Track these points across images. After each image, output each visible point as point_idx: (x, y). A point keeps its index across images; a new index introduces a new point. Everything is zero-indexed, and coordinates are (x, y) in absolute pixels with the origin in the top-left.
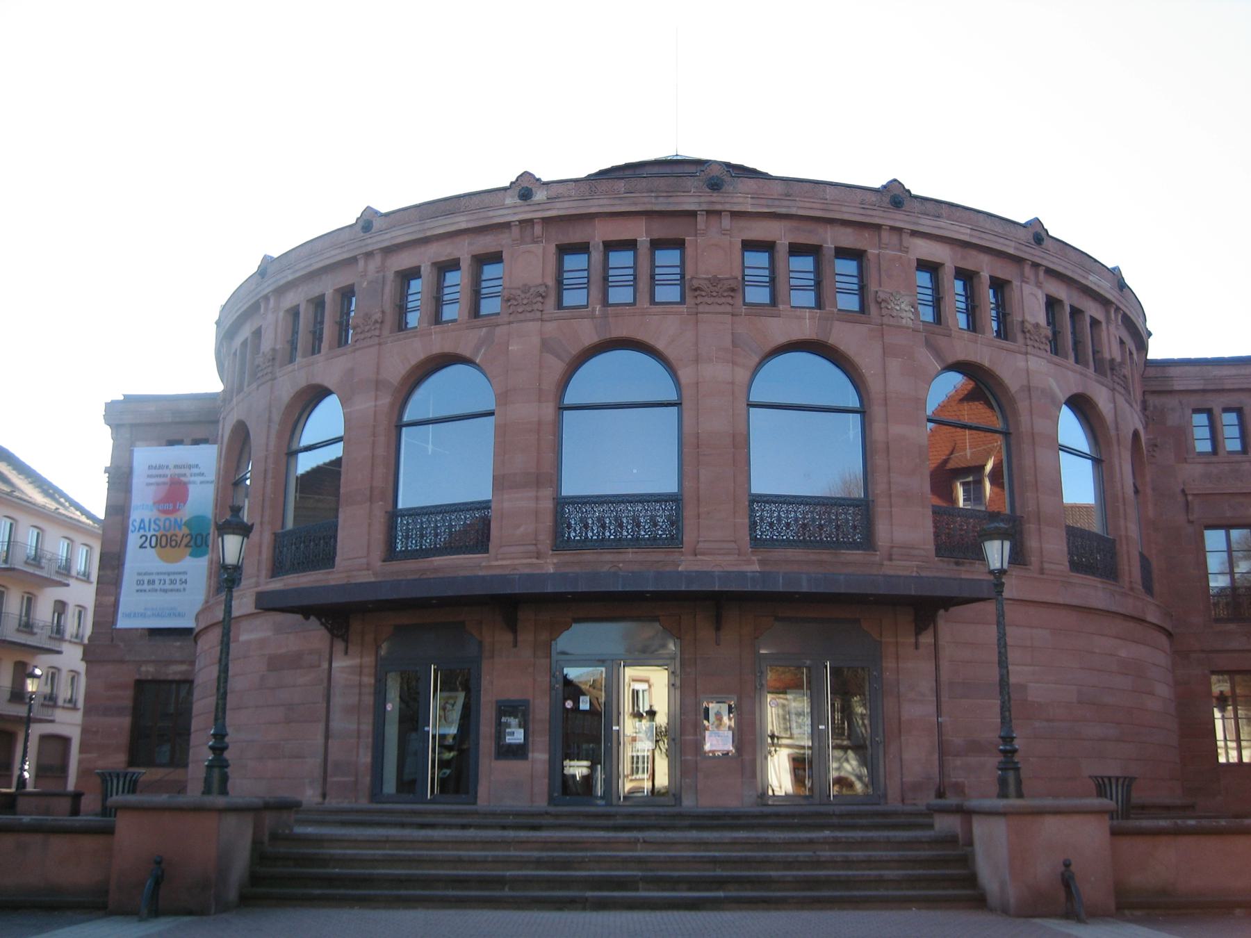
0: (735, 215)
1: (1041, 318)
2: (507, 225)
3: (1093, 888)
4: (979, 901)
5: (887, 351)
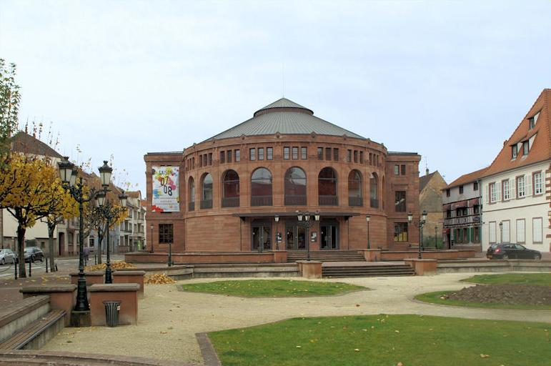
0: (317, 143)
1: (368, 158)
2: (274, 143)
3: (378, 259)
4: (365, 261)
5: (342, 168)
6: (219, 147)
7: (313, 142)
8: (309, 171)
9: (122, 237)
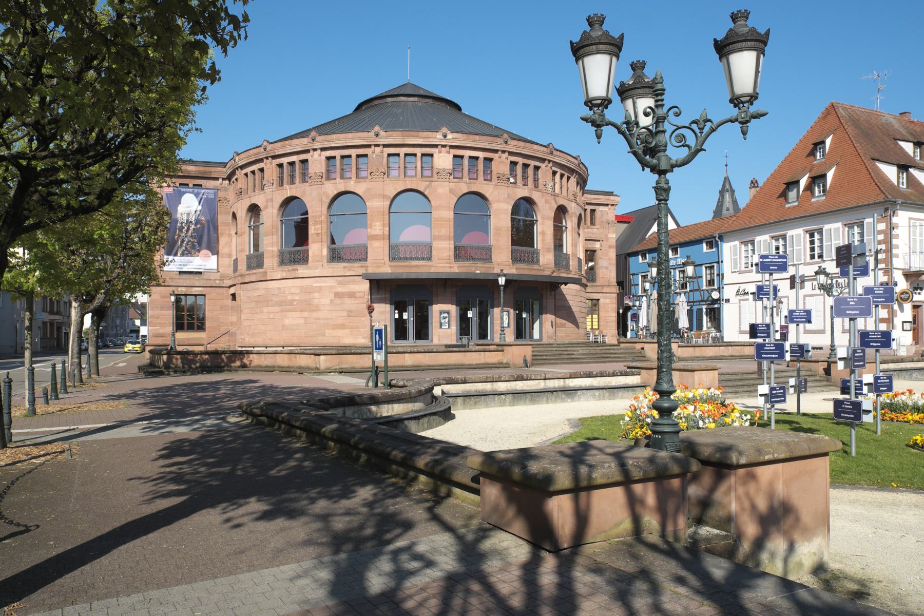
6: (323, 149)
7: (504, 152)
8: (499, 201)
9: (45, 323)
